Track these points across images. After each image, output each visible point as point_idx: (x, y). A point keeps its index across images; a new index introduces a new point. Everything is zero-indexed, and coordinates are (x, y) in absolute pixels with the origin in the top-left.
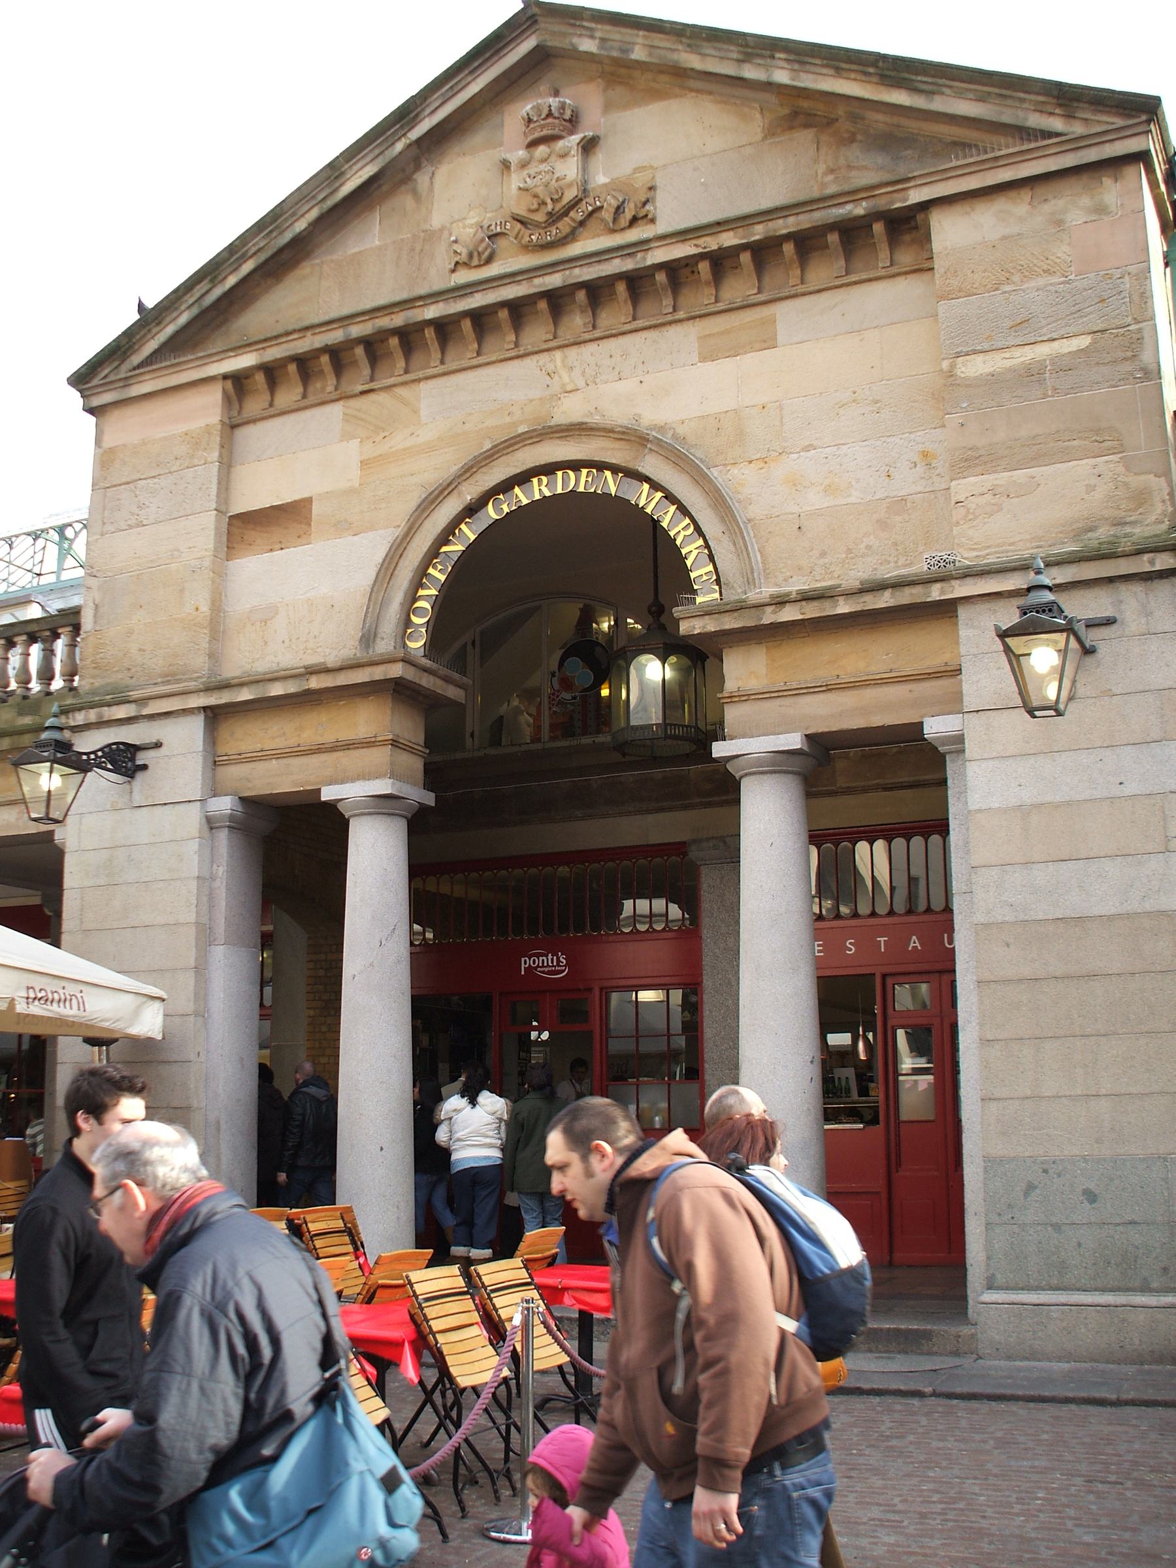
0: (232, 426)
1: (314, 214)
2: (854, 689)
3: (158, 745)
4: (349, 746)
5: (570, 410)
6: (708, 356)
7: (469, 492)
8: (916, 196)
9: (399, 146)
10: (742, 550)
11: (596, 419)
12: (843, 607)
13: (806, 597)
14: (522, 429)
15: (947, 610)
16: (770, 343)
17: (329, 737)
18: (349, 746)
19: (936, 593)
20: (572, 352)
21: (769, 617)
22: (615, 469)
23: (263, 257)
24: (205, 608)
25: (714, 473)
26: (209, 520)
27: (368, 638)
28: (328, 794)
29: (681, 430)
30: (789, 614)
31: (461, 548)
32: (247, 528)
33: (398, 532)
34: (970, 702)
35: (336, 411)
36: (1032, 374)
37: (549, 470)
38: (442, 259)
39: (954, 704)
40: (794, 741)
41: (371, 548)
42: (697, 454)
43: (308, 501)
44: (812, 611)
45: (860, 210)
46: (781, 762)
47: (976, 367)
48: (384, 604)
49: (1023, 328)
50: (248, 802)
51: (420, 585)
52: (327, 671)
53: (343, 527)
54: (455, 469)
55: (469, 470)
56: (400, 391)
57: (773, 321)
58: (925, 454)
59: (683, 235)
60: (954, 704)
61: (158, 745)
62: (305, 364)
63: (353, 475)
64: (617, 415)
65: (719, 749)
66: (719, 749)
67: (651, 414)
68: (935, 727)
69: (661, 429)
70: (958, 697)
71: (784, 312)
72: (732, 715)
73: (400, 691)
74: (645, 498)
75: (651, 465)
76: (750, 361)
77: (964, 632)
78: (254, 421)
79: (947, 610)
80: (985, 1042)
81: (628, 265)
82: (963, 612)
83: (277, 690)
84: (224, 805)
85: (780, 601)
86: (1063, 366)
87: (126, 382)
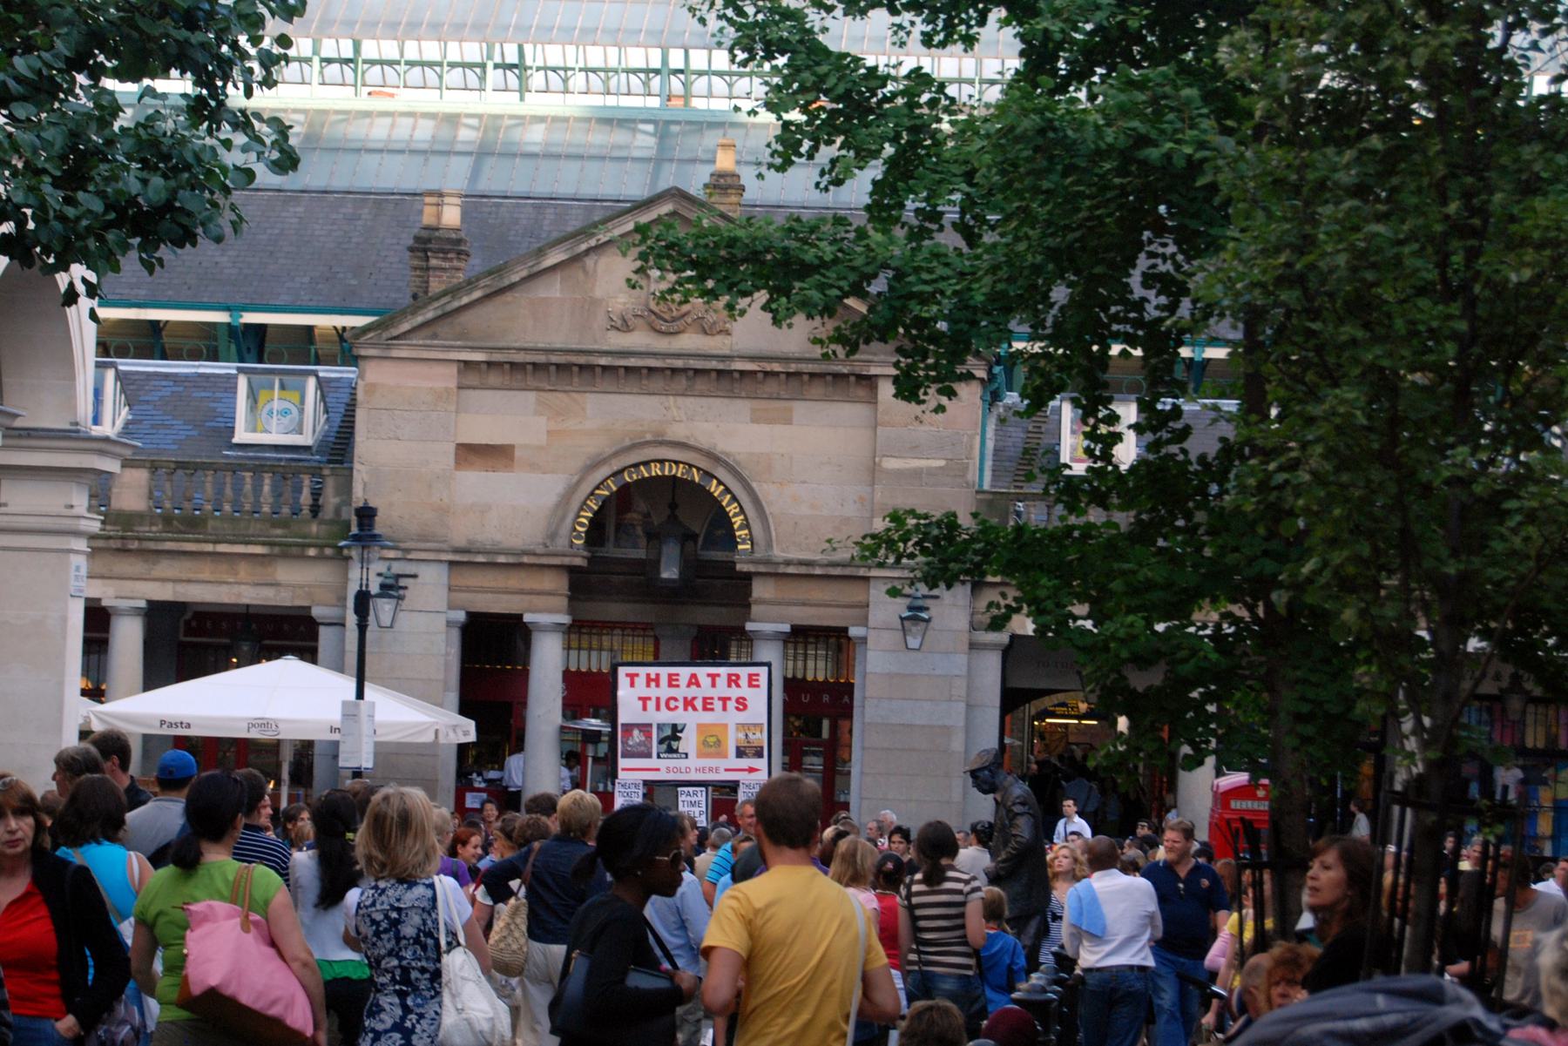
0: (459, 388)
1: (524, 273)
2: (820, 607)
3: (415, 576)
4: (539, 593)
5: (678, 432)
6: (755, 420)
7: (616, 465)
8: (874, 371)
9: (584, 247)
10: (767, 528)
11: (692, 442)
12: (818, 571)
13: (801, 563)
14: (649, 437)
16: (789, 422)
18: (539, 593)
20: (680, 400)
21: (782, 569)
22: (699, 469)
23: (488, 291)
25: (754, 485)
26: (452, 448)
27: (553, 536)
28: (527, 618)
29: (738, 458)
30: (791, 570)
31: (606, 493)
32: (471, 453)
33: (576, 478)
34: (871, 623)
35: (532, 396)
36: (917, 474)
37: (662, 462)
38: (601, 320)
39: (864, 622)
40: (786, 628)
42: (745, 473)
43: (512, 447)
44: (803, 570)
45: (845, 371)
46: (778, 636)
47: (891, 464)
48: (563, 518)
49: (915, 450)
50: (470, 615)
51: (581, 509)
52: (535, 554)
53: (533, 467)
54: (609, 451)
55: (616, 454)
56: (574, 395)
57: (791, 410)
58: (861, 498)
59: (752, 359)
61: (415, 576)
62: (514, 366)
63: (542, 439)
64: (704, 442)
67: (722, 445)
68: (854, 631)
69: (727, 454)
70: (866, 618)
71: (799, 408)
72: (755, 609)
73: (572, 570)
74: (715, 489)
75: (721, 473)
76: (779, 429)
78: (474, 388)
79: (866, 579)
80: (862, 773)
81: (721, 366)
82: (872, 583)
83: (502, 559)
84: (461, 616)
85: (788, 563)
86: (931, 472)
87: (389, 347)
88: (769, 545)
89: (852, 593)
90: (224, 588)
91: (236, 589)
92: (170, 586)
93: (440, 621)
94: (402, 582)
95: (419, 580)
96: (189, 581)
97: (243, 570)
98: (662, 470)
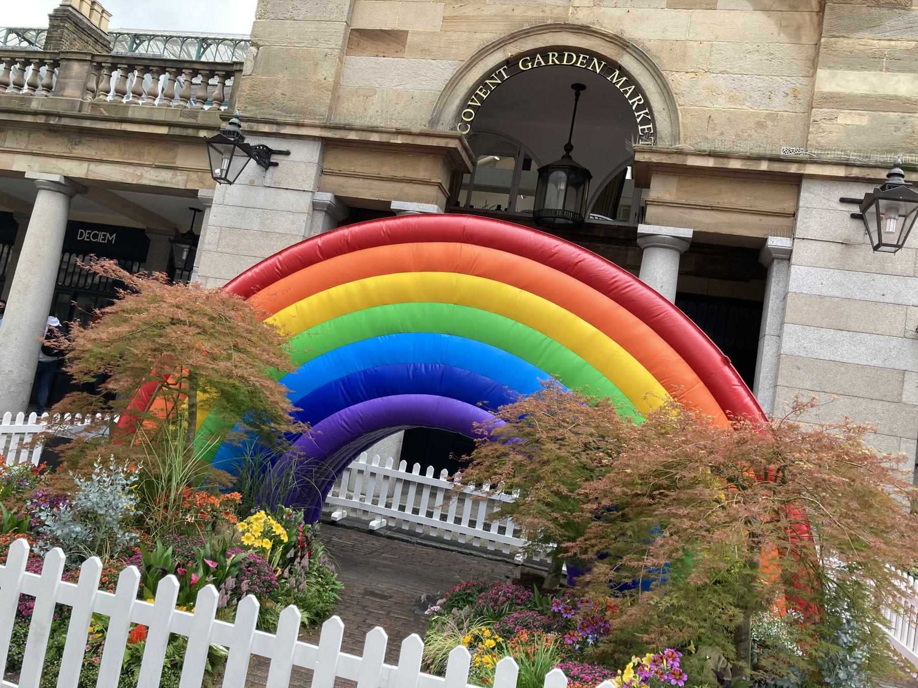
3: (287, 153)
15: (795, 182)
17: (399, 174)
18: (411, 181)
19: (793, 169)
24: (331, 80)
27: (433, 122)
34: (799, 233)
39: (790, 232)
40: (688, 233)
41: (444, 70)
60: (790, 232)
61: (287, 153)
65: (642, 229)
66: (642, 229)
68: (775, 242)
72: (650, 211)
75: (628, 62)
77: (803, 194)
82: (805, 184)
88: (676, 137)
89: (773, 199)
90: (130, 170)
91: (139, 171)
92: (85, 165)
93: (305, 201)
94: (274, 158)
95: (291, 157)
96: (101, 161)
97: (152, 154)
98: (561, 58)
